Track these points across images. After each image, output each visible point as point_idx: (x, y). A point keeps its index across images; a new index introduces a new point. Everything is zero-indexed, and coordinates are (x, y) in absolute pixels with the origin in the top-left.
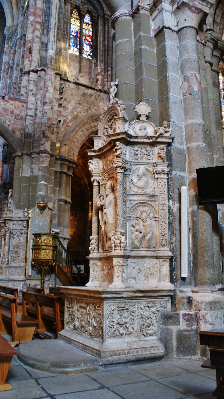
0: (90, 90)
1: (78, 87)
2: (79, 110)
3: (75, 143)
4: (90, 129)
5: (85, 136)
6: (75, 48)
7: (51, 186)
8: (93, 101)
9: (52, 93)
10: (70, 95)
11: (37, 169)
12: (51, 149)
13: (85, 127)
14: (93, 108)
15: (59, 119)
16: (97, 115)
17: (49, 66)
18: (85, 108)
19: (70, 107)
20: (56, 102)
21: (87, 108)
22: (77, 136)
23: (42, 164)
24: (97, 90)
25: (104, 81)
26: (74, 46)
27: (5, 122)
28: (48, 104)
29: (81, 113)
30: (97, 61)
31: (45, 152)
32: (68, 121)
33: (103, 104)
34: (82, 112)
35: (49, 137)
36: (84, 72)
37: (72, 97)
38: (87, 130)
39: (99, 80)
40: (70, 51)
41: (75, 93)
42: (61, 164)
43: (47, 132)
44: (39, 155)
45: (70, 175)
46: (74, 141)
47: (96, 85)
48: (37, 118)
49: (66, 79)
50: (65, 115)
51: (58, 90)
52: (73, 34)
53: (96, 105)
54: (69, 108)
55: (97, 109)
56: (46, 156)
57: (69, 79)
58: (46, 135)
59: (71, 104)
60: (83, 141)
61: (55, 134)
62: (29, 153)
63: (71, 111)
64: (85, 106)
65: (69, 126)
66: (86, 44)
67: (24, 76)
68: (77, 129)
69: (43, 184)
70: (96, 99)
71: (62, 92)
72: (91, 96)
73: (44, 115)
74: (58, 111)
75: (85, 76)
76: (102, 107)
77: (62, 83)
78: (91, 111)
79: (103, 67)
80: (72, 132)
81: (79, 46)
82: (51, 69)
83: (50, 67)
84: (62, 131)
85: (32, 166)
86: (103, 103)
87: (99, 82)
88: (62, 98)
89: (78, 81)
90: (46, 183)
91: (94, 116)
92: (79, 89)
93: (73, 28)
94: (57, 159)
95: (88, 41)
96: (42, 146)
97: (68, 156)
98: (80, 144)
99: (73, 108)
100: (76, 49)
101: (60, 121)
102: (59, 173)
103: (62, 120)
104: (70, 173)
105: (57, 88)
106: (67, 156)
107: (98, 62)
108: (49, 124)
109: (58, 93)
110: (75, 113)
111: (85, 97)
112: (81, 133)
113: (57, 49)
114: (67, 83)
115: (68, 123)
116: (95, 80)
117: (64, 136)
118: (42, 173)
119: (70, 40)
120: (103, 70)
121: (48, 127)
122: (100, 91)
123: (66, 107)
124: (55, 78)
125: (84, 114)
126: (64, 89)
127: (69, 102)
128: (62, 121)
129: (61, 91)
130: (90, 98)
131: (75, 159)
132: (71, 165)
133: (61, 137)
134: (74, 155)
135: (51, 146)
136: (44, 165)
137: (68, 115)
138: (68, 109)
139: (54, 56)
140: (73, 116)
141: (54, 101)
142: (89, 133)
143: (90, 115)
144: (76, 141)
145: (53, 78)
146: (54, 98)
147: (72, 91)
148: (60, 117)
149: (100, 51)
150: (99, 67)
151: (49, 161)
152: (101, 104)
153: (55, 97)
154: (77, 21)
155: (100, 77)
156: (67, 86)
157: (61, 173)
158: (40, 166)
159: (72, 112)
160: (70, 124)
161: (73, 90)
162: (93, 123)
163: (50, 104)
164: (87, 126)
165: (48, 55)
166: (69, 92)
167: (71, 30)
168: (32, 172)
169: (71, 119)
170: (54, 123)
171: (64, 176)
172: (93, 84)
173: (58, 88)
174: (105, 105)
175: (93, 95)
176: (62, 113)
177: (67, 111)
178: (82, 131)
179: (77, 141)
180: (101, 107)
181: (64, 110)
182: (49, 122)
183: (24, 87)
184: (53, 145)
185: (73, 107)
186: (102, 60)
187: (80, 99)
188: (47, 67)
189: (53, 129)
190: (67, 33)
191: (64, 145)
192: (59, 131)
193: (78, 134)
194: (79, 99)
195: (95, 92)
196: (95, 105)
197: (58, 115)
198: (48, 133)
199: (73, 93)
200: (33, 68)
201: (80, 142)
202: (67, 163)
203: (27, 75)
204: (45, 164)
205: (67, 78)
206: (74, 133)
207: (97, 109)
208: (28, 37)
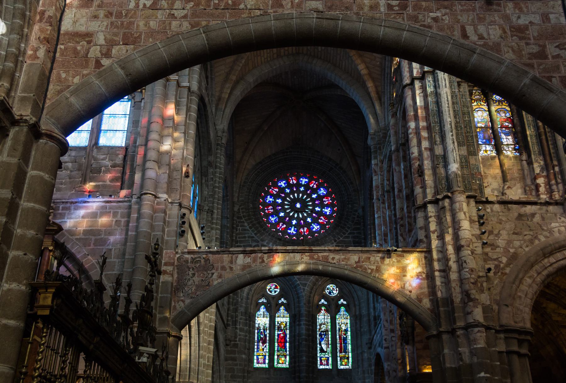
0: (529, 207)
1: (508, 206)
2: (517, 244)
3: (523, 299)
4: (543, 271)
5: (537, 285)
6: (487, 146)
7: (496, 378)
8: (538, 223)
9: (469, 228)
10: (497, 223)
11: (467, 354)
12: (485, 318)
13: (534, 268)
14: (541, 234)
15: (487, 266)
16: (551, 245)
17: (456, 188)
18: (527, 238)
19: (501, 242)
20: (476, 241)
21: (530, 237)
22: (524, 287)
23: (475, 344)
24: (541, 204)
25: (550, 186)
26: (485, 143)
27: (404, 288)
28: (465, 247)
29: (521, 247)
30: (529, 156)
31: (477, 325)
32: (502, 265)
33: (557, 224)
34: (524, 247)
35: (478, 300)
36: (511, 180)
37: (501, 226)
38: (539, 273)
39: (540, 186)
40: (482, 153)
41: (504, 219)
42: (506, 338)
43: (473, 292)
44: (467, 331)
45: (524, 355)
46: (520, 297)
47: (538, 195)
48: (453, 272)
49: (484, 199)
50: (495, 257)
51: (476, 222)
52: (479, 125)
53: (545, 228)
54: (501, 245)
55: (548, 235)
56: (479, 331)
57: (490, 199)
58: (472, 297)
59: (501, 237)
60: (535, 293)
61: (486, 292)
62: (450, 330)
63: (504, 248)
64: (526, 235)
65: (506, 274)
66: (506, 134)
67: (418, 212)
68: (521, 276)
69: (483, 377)
70: (543, 218)
71: (483, 223)
72: (533, 215)
73: (462, 266)
74: (482, 254)
75: (515, 185)
76: (556, 230)
77: (480, 208)
78: (539, 240)
79: (542, 163)
80: (513, 283)
81: (493, 140)
82: (459, 193)
83: (457, 191)
84: (497, 284)
85: (459, 349)
86: (557, 222)
87: (542, 189)
88: (485, 232)
89: (505, 198)
90: (488, 375)
91: (545, 248)
92: (509, 210)
93: (479, 117)
94: (497, 332)
95: (507, 127)
96: (470, 316)
97: (516, 322)
98: (531, 299)
99: (507, 243)
100: (489, 148)
101: (489, 270)
102: (505, 354)
103: (492, 267)
104: (524, 351)
105: (473, 218)
106: (513, 323)
107: (533, 156)
108: (473, 278)
109: (477, 226)
110: (512, 251)
111: (524, 220)
112: (529, 281)
113: (461, 159)
114: (488, 206)
115: (503, 269)
116: (533, 187)
117: (501, 293)
118: (478, 359)
119: (477, 136)
120: (544, 167)
121: (473, 283)
122: (547, 204)
123: (495, 244)
124: (468, 204)
125: (527, 249)
126: (485, 218)
127: (498, 235)
128: (493, 268)
129: (482, 221)
130: (532, 220)
131: (528, 325)
132: (523, 337)
133: (495, 295)
134: (523, 319)
135: (484, 312)
136: (479, 346)
137: (500, 256)
138: (499, 247)
139: (459, 172)
140: (509, 257)
141: (474, 240)
142: (543, 278)
143: (539, 248)
144: (523, 296)
145: (465, 205)
146: (472, 235)
147: (499, 215)
148: (489, 262)
149: (531, 138)
150: (536, 165)
151: (485, 338)
152: (553, 225)
153: (474, 233)
154: (482, 103)
155: (541, 181)
156: (489, 210)
157: (509, 353)
158: (472, 347)
159: (506, 250)
160: (508, 270)
161: (501, 214)
162: (546, 260)
163: (469, 247)
164: (537, 267)
165: (450, 172)
166: (495, 219)
167: (476, 120)
168: (461, 359)
169: (507, 261)
170: (481, 274)
171: (515, 358)
172: (531, 194)
173: (476, 219)
174: (562, 224)
175: (535, 214)
176: (490, 254)
177: (498, 250)
178: (530, 277)
179: (526, 295)
180: (555, 230)
181: (492, 249)
182: (473, 276)
183: (421, 228)
184: (486, 310)
185: (506, 242)
186: (539, 152)
187: (515, 225)
188: (451, 191)
189: (482, 285)
190: (471, 127)
191: (505, 307)
192: (491, 286)
193: (524, 283)
194: (513, 225)
195: (538, 207)
196: (543, 229)
197: (485, 261)
198: (474, 293)
199: (501, 220)
200: (429, 197)
201: (530, 296)
202: (517, 336)
203: (423, 210)
204: (479, 344)
205: (487, 198)
206: (517, 283)
207: (548, 235)
208: (413, 153)
